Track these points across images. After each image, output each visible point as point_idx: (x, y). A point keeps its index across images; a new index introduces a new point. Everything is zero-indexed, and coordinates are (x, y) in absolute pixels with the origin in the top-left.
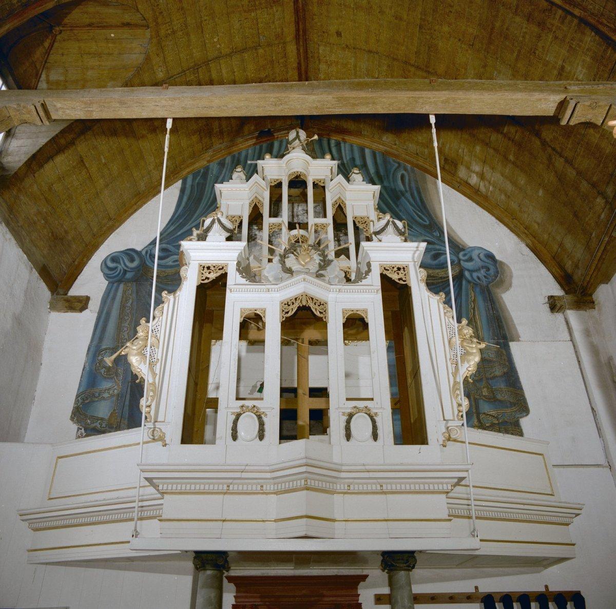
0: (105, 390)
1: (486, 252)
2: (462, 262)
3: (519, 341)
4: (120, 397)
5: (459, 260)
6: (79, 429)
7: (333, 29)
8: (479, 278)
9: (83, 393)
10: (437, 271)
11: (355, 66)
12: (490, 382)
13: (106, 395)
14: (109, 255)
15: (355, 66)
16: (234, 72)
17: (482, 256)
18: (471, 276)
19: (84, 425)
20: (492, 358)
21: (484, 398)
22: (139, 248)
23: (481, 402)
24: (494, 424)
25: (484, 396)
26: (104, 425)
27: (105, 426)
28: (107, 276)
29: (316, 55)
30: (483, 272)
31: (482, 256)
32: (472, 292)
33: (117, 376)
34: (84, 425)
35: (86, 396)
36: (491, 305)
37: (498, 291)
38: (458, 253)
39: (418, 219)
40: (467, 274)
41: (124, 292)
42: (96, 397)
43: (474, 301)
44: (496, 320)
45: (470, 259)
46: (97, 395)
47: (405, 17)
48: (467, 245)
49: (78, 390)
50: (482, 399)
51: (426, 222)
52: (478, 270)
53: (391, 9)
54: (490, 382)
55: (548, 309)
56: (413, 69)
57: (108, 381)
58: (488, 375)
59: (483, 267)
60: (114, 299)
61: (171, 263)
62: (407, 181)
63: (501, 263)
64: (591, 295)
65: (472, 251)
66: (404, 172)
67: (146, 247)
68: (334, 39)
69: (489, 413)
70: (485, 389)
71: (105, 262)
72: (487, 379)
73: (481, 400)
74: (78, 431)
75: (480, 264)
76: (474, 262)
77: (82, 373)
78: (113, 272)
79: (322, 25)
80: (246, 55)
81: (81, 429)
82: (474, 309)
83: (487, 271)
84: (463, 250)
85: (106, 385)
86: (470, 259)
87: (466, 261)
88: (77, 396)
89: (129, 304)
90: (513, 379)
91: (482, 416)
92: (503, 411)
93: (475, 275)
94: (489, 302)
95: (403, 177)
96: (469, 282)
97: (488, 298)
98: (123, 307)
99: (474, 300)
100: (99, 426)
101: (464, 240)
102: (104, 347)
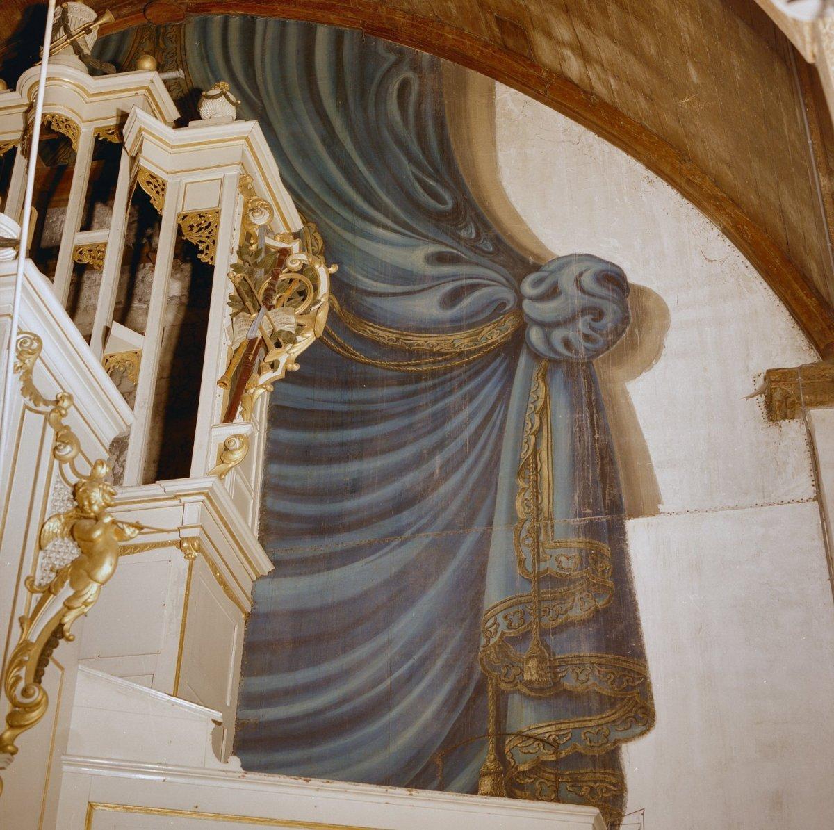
1: (601, 267)
3: (656, 512)
5: (520, 298)
8: (567, 344)
10: (451, 337)
12: (551, 640)
17: (587, 280)
18: (548, 340)
20: (568, 570)
21: (525, 690)
23: (515, 701)
24: (544, 763)
25: (527, 684)
30: (582, 324)
31: (587, 280)
32: (542, 385)
36: (592, 416)
37: (618, 373)
38: (520, 280)
40: (535, 335)
43: (543, 412)
44: (598, 460)
45: (553, 292)
48: (550, 253)
50: (519, 692)
51: (445, 203)
52: (569, 321)
54: (551, 640)
58: (548, 622)
59: (584, 311)
62: (413, 97)
63: (641, 292)
65: (561, 268)
66: (410, 74)
69: (533, 733)
70: (533, 663)
72: (544, 632)
73: (517, 697)
75: (578, 300)
76: (562, 298)
83: (594, 320)
84: (537, 268)
86: (553, 292)
87: (541, 298)
90: (621, 627)
91: (510, 743)
92: (577, 725)
93: (558, 335)
94: (585, 408)
95: (405, 85)
96: (536, 356)
97: (585, 400)
99: (545, 406)
101: (543, 240)
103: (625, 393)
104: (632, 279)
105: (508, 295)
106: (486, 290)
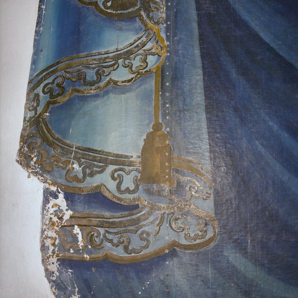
0: (118, 57)
6: (48, 195)
9: (49, 70)
13: (121, 75)
19: (62, 181)
26: (128, 182)
27: (132, 187)
33: (148, 10)
34: (62, 181)
35: (59, 80)
42: (92, 84)
46: (91, 75)
49: (34, 62)
57: (121, 29)
74: (46, 201)
77: (40, 9)
81: (56, 197)
100: (112, 185)
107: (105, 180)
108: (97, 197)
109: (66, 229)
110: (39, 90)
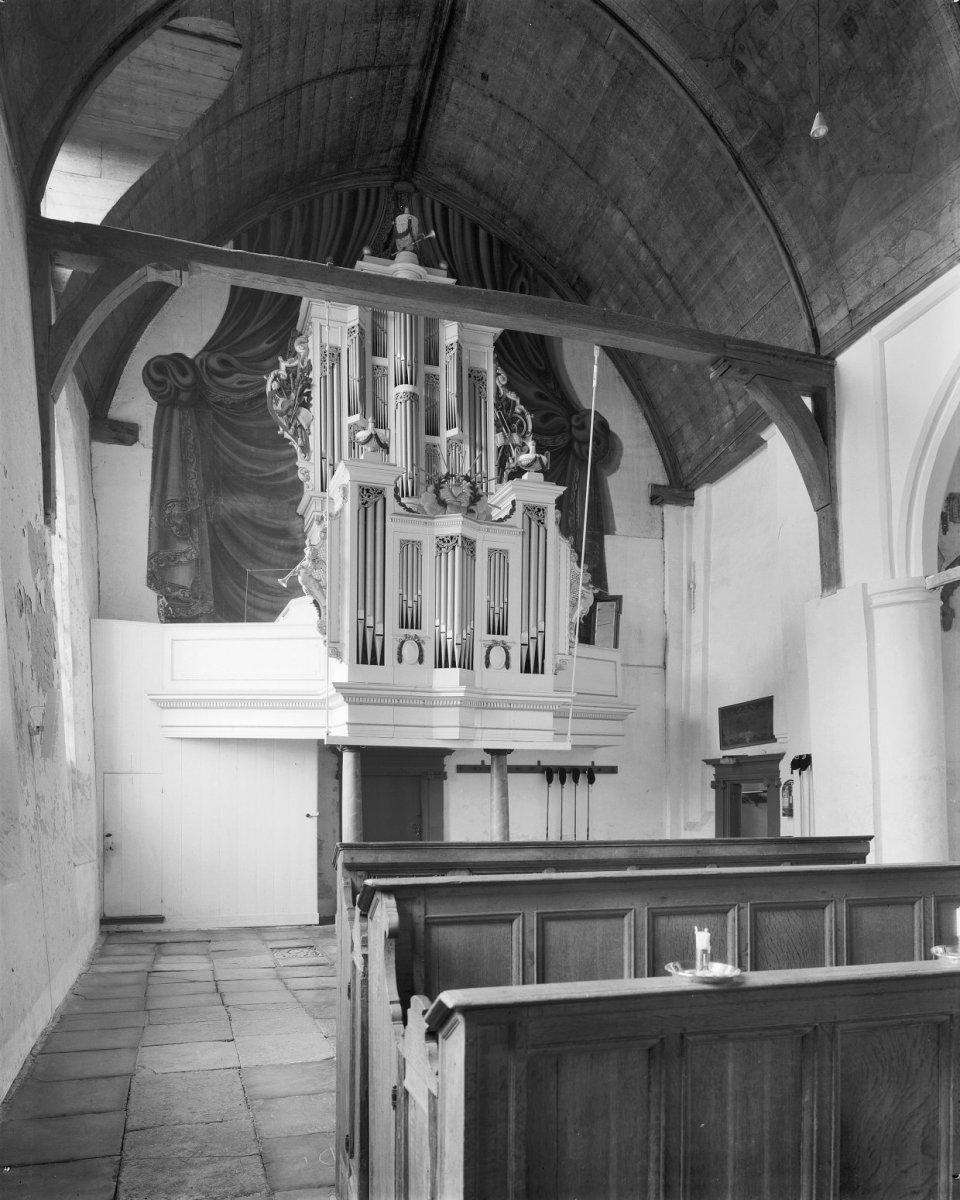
2: (573, 430)
3: (614, 534)
4: (199, 562)
5: (571, 426)
6: (159, 598)
7: (478, 68)
9: (156, 554)
11: (495, 124)
13: (183, 559)
14: (152, 360)
15: (495, 124)
16: (331, 98)
18: (580, 448)
22: (190, 355)
28: (153, 393)
29: (445, 91)
38: (571, 416)
39: (533, 360)
41: (181, 421)
47: (579, 97)
49: (149, 550)
53: (563, 77)
55: (649, 500)
56: (569, 161)
60: (169, 431)
61: (235, 385)
64: (694, 491)
66: (524, 280)
67: (199, 354)
68: (476, 80)
71: (146, 371)
78: (161, 389)
79: (465, 58)
80: (352, 78)
82: (576, 491)
85: (183, 547)
87: (578, 428)
88: (149, 560)
89: (190, 441)
98: (183, 445)
102: (169, 498)
103: (606, 480)
104: (612, 428)
105: (567, 423)
106: (555, 419)
107: (179, 593)
108: (177, 598)
109: (166, 609)
110: (152, 561)
